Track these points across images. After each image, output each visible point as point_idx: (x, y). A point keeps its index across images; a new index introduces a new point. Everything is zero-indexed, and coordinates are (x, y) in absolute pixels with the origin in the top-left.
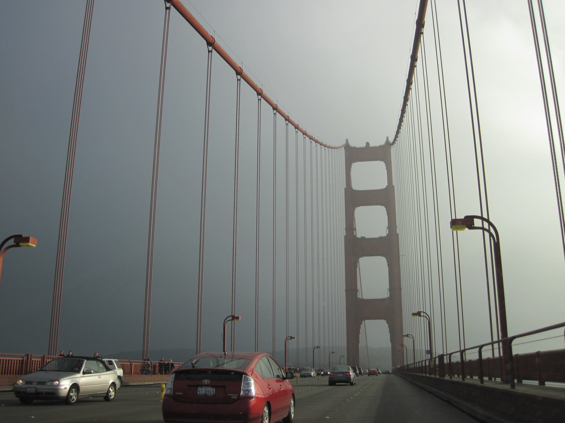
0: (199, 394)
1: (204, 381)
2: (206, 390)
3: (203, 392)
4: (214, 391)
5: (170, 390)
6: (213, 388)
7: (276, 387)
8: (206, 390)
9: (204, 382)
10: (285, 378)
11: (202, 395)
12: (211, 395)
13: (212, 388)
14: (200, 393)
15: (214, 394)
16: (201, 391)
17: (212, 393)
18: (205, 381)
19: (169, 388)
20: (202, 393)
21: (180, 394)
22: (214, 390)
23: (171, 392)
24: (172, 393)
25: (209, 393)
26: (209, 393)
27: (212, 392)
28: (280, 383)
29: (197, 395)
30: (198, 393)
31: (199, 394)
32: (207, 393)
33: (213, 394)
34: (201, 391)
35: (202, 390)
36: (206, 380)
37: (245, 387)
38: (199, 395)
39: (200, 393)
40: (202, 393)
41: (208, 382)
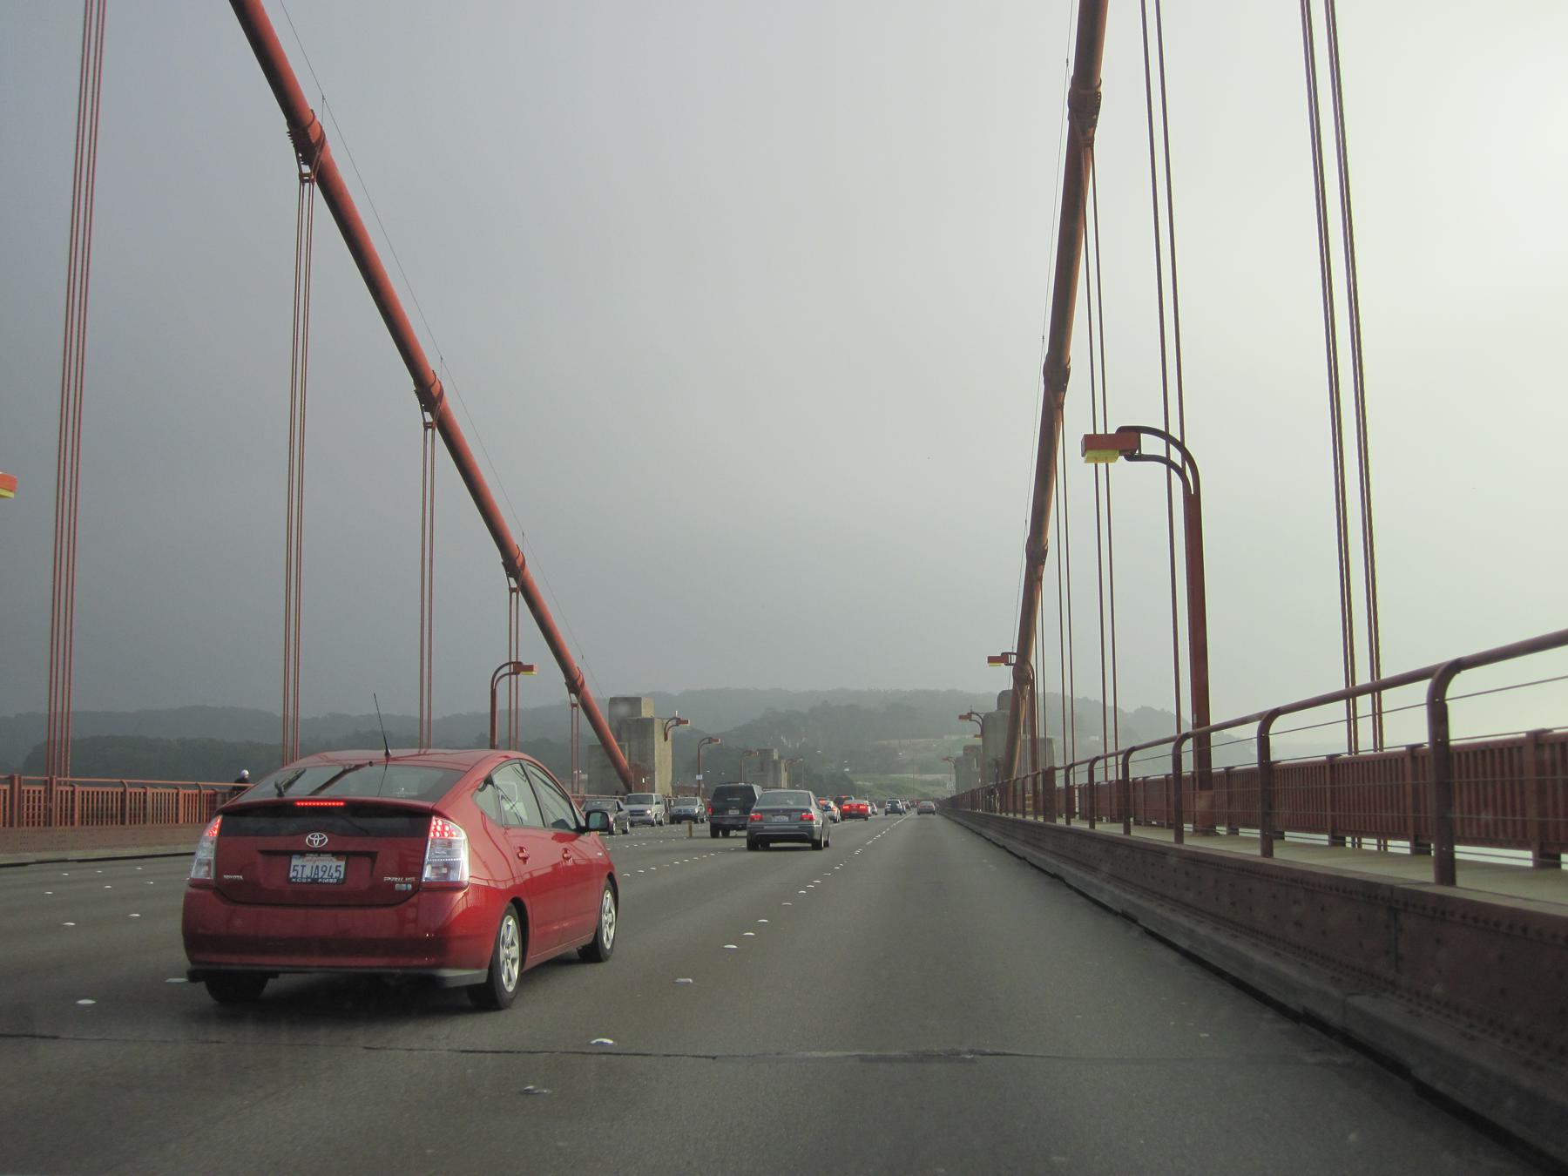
0: (294, 877)
1: (310, 836)
2: (317, 867)
3: (307, 872)
4: (342, 869)
5: (206, 868)
6: (338, 860)
7: (546, 855)
8: (317, 867)
9: (311, 841)
10: (584, 828)
11: (304, 881)
12: (331, 881)
13: (334, 859)
14: (299, 876)
15: (342, 877)
16: (300, 869)
17: (337, 875)
18: (314, 839)
19: (206, 862)
20: (304, 876)
21: (237, 879)
22: (343, 863)
23: (208, 872)
24: (212, 878)
25: (326, 876)
26: (326, 876)
27: (337, 871)
28: (565, 845)
29: (289, 880)
30: (291, 876)
31: (296, 878)
32: (321, 874)
33: (338, 879)
34: (300, 869)
35: (303, 866)
36: (317, 834)
37: (437, 854)
38: (294, 880)
39: (299, 876)
40: (304, 876)
41: (321, 842)
